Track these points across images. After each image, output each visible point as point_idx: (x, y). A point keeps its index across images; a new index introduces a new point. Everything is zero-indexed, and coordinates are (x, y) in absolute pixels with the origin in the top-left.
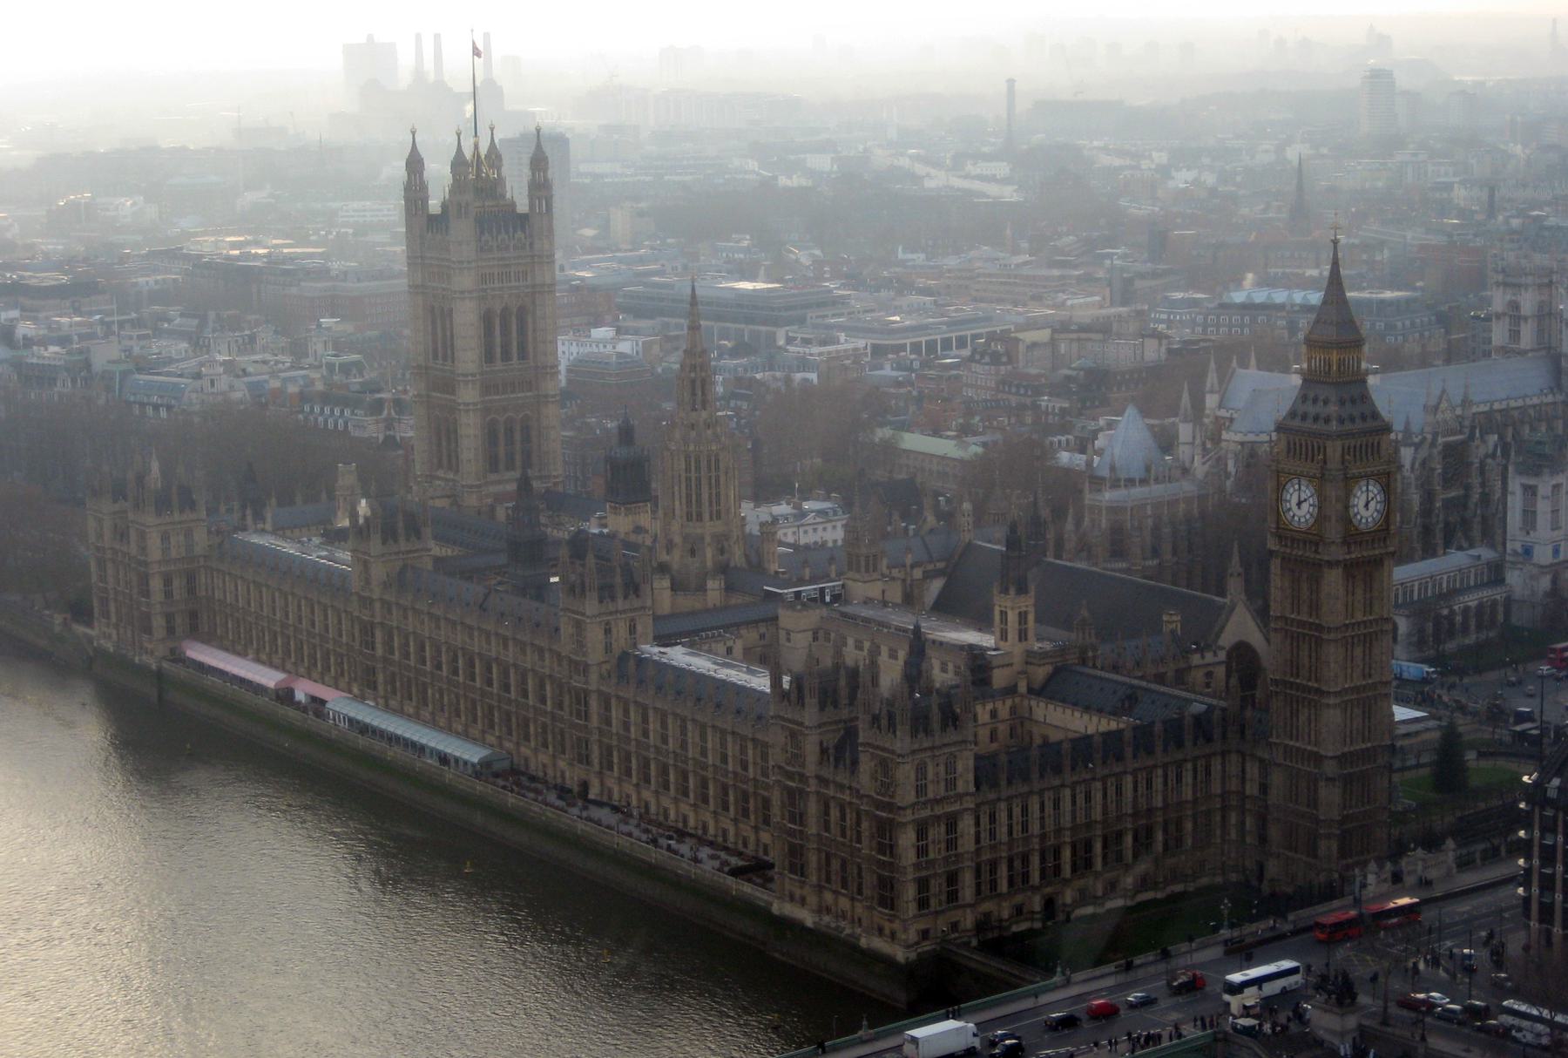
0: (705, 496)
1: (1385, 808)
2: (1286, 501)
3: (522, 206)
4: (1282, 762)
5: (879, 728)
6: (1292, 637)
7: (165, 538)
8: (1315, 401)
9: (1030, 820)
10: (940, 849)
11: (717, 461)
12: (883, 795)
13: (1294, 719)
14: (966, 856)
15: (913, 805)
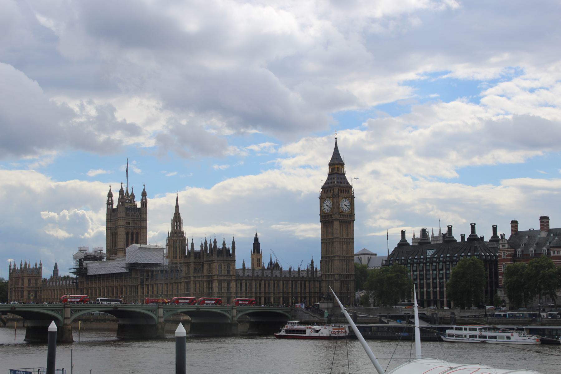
0: (178, 251)
1: (353, 292)
2: (324, 206)
3: (139, 206)
4: (325, 280)
5: (209, 256)
6: (327, 244)
7: (29, 281)
8: (331, 179)
9: (252, 288)
10: (225, 289)
11: (182, 243)
12: (210, 274)
13: (328, 267)
14: (233, 293)
15: (218, 275)
